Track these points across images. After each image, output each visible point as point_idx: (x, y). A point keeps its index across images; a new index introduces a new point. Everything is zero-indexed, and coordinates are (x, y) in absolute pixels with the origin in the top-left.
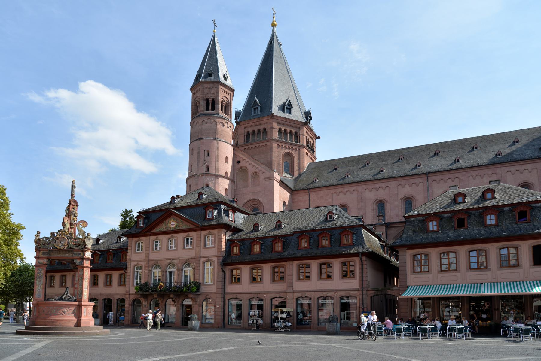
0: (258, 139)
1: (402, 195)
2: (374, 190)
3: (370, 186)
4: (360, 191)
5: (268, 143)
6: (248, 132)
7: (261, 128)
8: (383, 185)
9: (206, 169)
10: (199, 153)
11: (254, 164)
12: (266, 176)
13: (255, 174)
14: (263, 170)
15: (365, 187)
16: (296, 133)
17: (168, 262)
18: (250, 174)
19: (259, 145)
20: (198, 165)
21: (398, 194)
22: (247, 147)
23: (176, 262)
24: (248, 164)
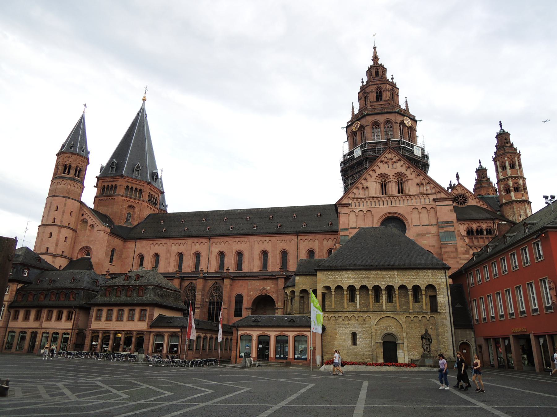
1: (193, 251)
3: (175, 242)
5: (116, 198)
6: (104, 186)
7: (114, 184)
8: (183, 241)
9: (52, 220)
10: (50, 207)
11: (92, 218)
12: (99, 229)
13: (92, 226)
14: (98, 224)
15: (172, 241)
16: (140, 190)
18: (89, 225)
20: (48, 217)
22: (101, 198)
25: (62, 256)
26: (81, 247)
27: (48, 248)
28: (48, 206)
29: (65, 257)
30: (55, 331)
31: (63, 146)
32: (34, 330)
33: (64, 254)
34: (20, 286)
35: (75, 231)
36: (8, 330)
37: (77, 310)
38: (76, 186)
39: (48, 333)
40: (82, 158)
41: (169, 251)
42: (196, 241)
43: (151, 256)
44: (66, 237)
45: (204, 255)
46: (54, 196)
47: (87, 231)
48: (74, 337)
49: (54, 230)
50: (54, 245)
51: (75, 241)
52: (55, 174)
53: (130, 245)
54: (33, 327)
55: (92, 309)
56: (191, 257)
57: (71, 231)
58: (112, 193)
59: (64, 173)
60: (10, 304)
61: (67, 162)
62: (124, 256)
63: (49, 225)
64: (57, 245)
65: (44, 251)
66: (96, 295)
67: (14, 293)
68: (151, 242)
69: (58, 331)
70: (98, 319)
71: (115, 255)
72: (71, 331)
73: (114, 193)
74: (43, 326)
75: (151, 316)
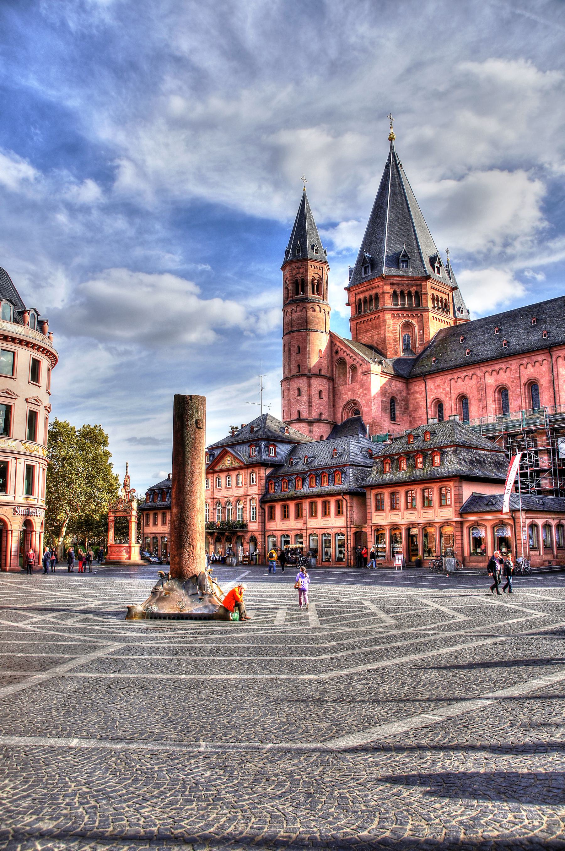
0: (371, 307)
1: (524, 380)
2: (494, 373)
3: (489, 369)
4: (479, 375)
5: (381, 315)
7: (373, 292)
10: (290, 350)
15: (484, 369)
16: (416, 292)
17: (226, 499)
19: (371, 317)
21: (520, 377)
22: (359, 321)
23: (231, 499)
24: (345, 354)
25: (319, 420)
26: (344, 403)
27: (299, 412)
28: (286, 349)
29: (325, 421)
30: (325, 531)
31: (287, 252)
32: (299, 532)
33: (324, 417)
34: (268, 471)
35: (331, 379)
36: (267, 534)
37: (347, 497)
38: (318, 309)
39: (316, 535)
40: (316, 264)
41: (482, 388)
42: (525, 361)
43: (453, 401)
44: (321, 392)
45: (544, 382)
46: (291, 332)
47: (348, 375)
48: (352, 537)
49: (302, 383)
50: (306, 405)
51: (334, 393)
52: (286, 298)
53: (416, 388)
54: (295, 527)
55: (368, 493)
56: (523, 392)
57: (325, 381)
58: (373, 307)
59: (298, 294)
60: (262, 498)
61: (298, 276)
62: (411, 407)
63: (294, 377)
64: (310, 405)
65: (295, 417)
66: (370, 473)
67: (263, 481)
68: (449, 377)
69: (329, 531)
70: (379, 508)
71: (397, 407)
72: (345, 529)
73: (376, 307)
74: (308, 526)
75: (459, 498)
